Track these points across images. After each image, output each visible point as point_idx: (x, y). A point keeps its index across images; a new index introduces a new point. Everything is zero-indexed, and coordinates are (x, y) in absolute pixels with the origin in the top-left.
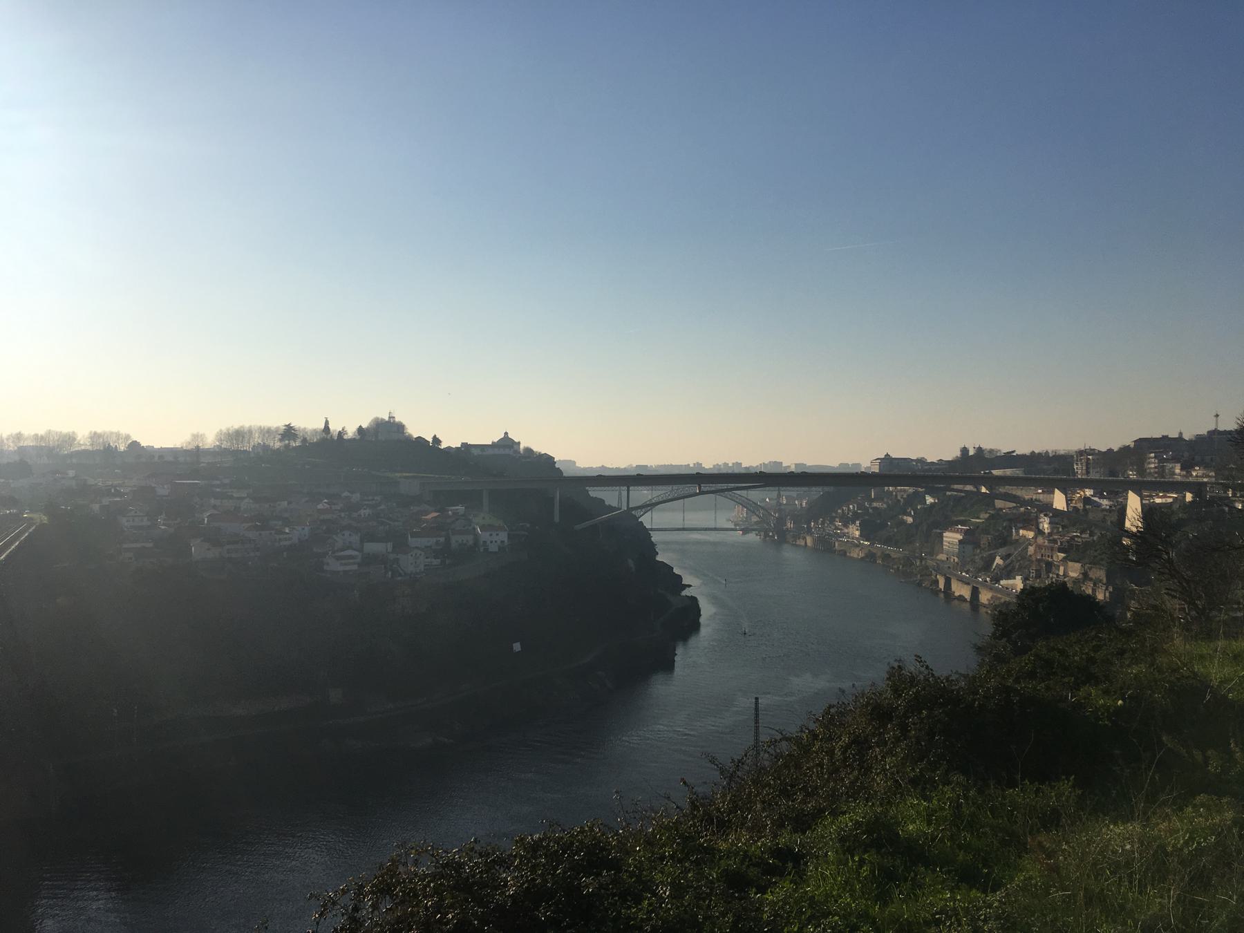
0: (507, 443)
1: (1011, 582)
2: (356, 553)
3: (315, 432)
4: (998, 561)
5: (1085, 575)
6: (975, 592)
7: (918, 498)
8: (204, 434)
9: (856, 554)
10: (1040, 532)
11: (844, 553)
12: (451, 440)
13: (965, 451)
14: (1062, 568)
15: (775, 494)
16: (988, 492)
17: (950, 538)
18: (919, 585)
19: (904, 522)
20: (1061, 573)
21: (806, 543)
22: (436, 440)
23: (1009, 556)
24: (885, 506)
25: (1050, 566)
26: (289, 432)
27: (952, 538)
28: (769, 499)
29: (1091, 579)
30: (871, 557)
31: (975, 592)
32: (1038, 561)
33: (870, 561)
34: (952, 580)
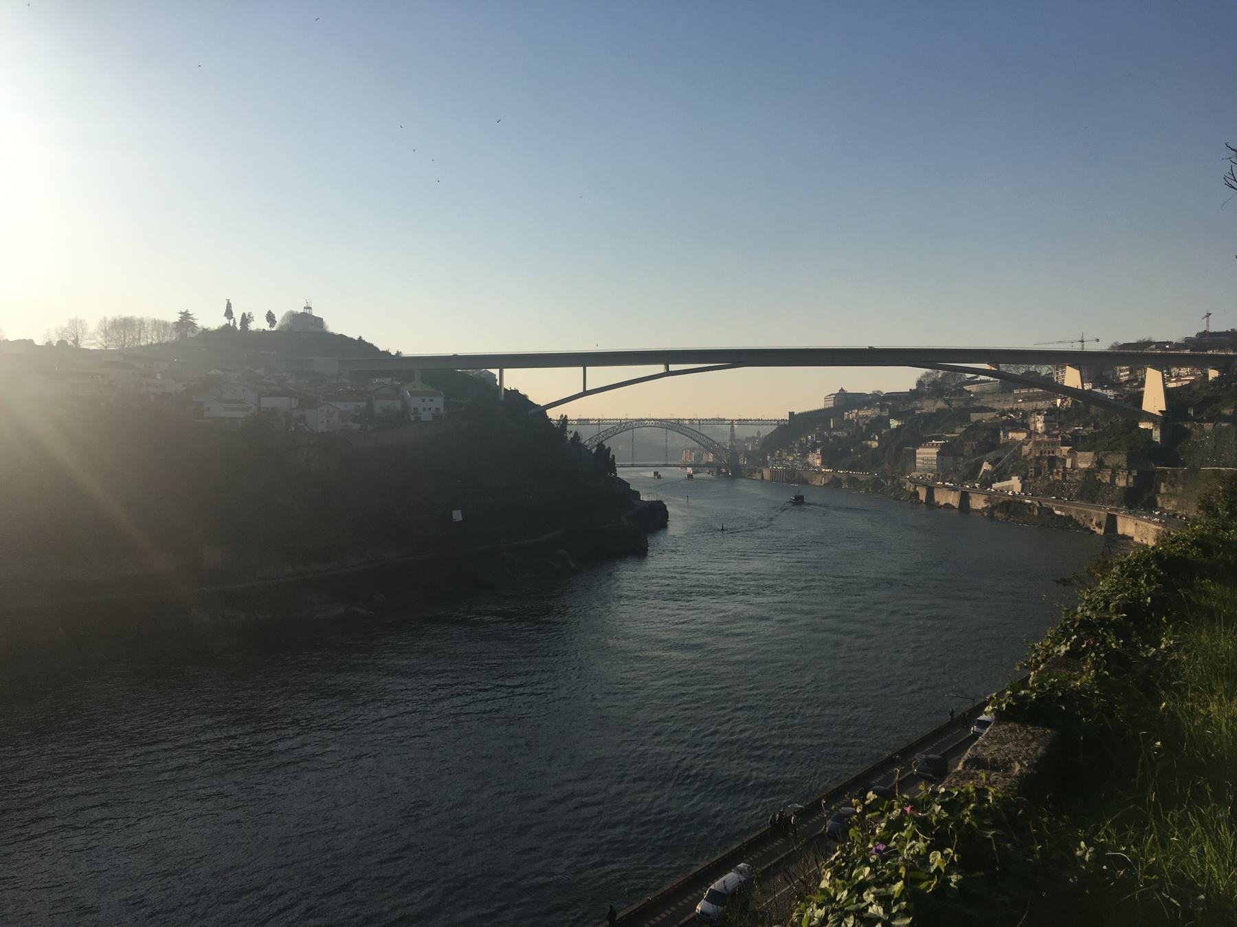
1: (1006, 483)
4: (986, 466)
5: (1100, 464)
6: (965, 498)
8: (84, 321)
9: (819, 481)
16: (993, 369)
17: (924, 454)
19: (868, 447)
20: (1068, 465)
21: (762, 476)
23: (998, 460)
24: (846, 434)
25: (1053, 461)
27: (927, 454)
29: (1107, 467)
30: (835, 483)
31: (965, 498)
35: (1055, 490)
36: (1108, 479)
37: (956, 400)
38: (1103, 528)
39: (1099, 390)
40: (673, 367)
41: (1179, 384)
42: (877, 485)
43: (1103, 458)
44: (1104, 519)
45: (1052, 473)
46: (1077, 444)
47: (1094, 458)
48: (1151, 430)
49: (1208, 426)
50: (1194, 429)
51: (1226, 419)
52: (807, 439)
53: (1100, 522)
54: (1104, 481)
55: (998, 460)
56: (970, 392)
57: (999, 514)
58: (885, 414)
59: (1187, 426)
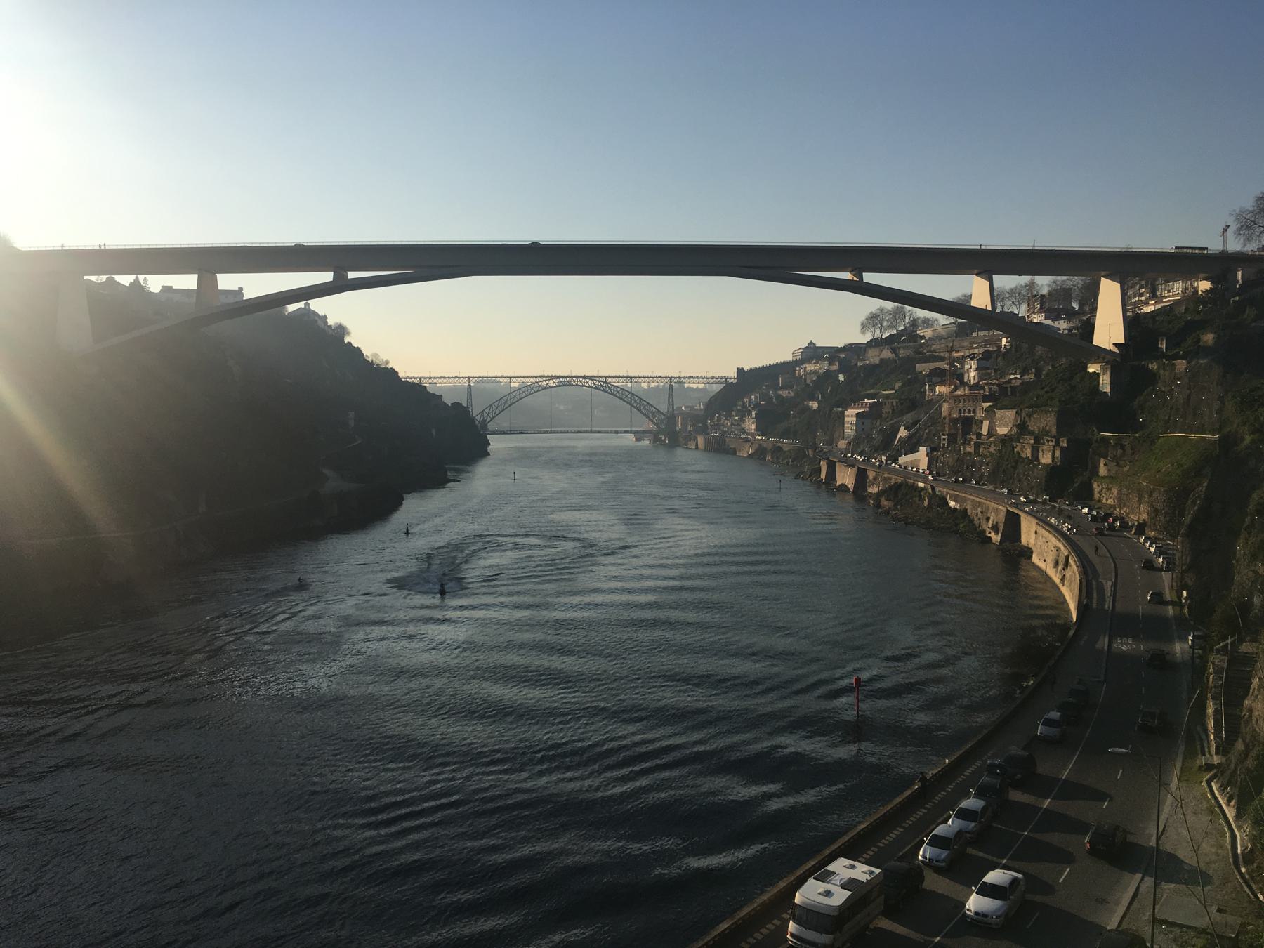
1: (911, 457)
4: (903, 433)
5: (1022, 428)
9: (747, 450)
14: (986, 424)
16: (855, 279)
19: (808, 408)
20: (985, 431)
21: (697, 445)
23: (915, 423)
24: (792, 394)
28: (685, 408)
29: (1031, 433)
30: (760, 454)
32: (955, 421)
33: (758, 458)
34: (837, 464)
35: (962, 471)
36: (1028, 452)
37: (904, 348)
38: (1000, 534)
39: (1049, 322)
40: (352, 275)
41: (1159, 306)
42: (799, 455)
43: (1027, 419)
44: (1002, 517)
45: (964, 444)
46: (1000, 398)
47: (1016, 420)
48: (1098, 375)
49: (1181, 365)
50: (1162, 372)
51: (1206, 351)
52: (750, 399)
53: (997, 523)
54: (1023, 455)
55: (915, 423)
56: (923, 337)
57: (886, 503)
58: (835, 367)
59: (1153, 366)
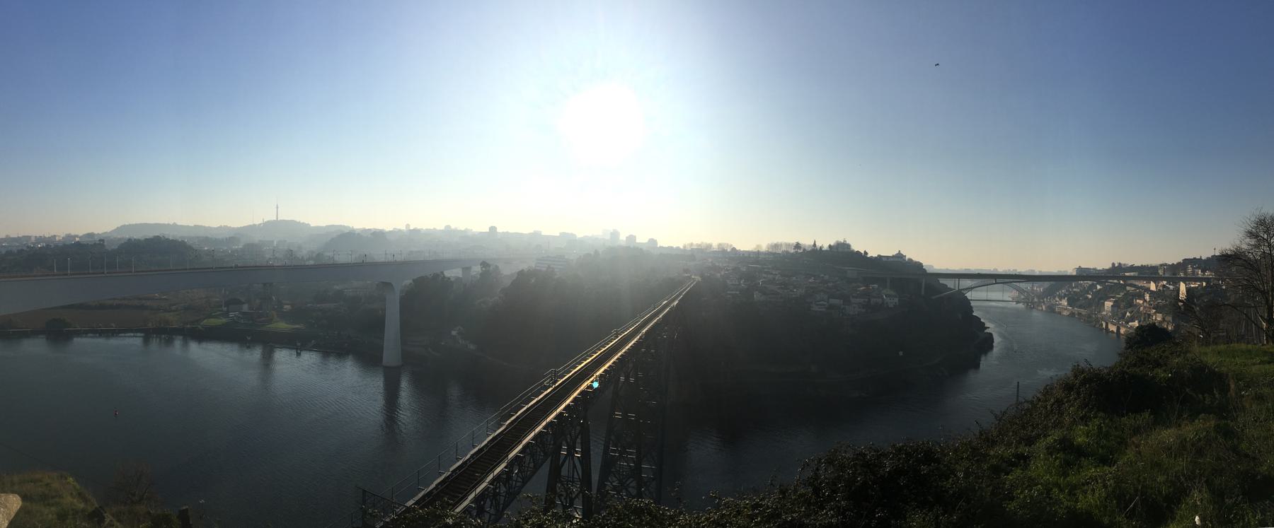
0: (900, 256)
1: (1133, 323)
2: (825, 303)
3: (810, 246)
4: (1128, 314)
6: (1118, 329)
7: (1093, 286)
9: (1065, 313)
10: (1145, 301)
11: (1060, 313)
12: (872, 253)
13: (1113, 264)
15: (1031, 285)
18: (1094, 326)
19: (1087, 298)
22: (866, 253)
26: (798, 246)
30: (1072, 315)
31: (1118, 329)
